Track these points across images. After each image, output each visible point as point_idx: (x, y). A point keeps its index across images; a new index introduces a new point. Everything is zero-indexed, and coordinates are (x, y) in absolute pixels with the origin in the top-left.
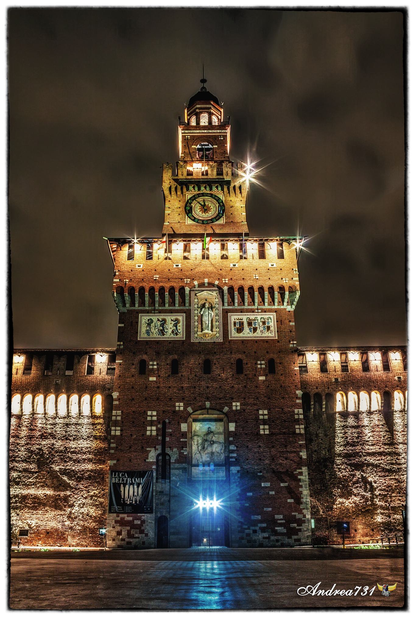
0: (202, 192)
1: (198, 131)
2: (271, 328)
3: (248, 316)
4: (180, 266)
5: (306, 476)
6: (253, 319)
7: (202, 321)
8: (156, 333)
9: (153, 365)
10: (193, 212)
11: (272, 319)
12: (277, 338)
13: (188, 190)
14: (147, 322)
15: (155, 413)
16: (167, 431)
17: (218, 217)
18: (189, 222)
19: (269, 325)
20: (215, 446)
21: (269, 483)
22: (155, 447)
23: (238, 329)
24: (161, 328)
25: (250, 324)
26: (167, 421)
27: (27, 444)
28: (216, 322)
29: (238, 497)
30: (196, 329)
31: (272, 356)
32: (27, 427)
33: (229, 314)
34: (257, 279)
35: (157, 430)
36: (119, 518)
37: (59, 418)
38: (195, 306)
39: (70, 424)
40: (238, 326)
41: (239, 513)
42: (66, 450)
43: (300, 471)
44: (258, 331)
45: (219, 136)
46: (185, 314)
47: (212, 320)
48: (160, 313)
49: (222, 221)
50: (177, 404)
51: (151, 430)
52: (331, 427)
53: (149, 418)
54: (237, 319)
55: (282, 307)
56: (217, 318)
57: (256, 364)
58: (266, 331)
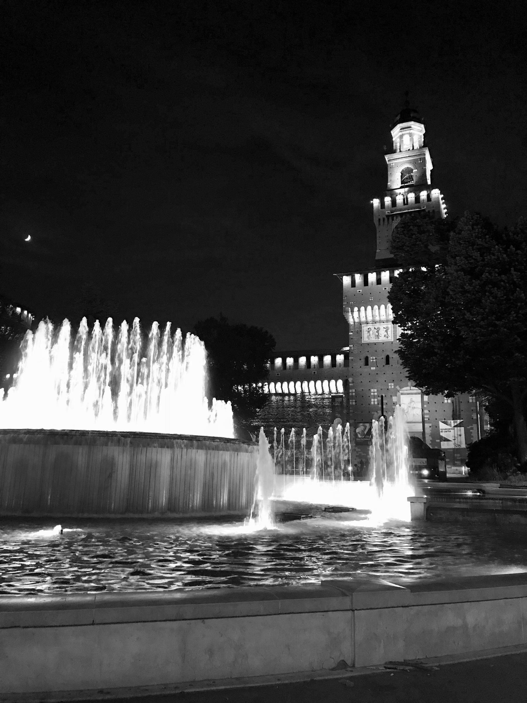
9: (373, 359)
14: (368, 330)
15: (376, 390)
20: (415, 410)
22: (377, 412)
24: (377, 334)
26: (384, 395)
27: (301, 411)
29: (431, 442)
32: (300, 401)
35: (378, 401)
37: (318, 395)
39: (325, 398)
42: (324, 414)
43: (472, 426)
45: (419, 160)
50: (390, 384)
51: (374, 401)
53: (372, 394)
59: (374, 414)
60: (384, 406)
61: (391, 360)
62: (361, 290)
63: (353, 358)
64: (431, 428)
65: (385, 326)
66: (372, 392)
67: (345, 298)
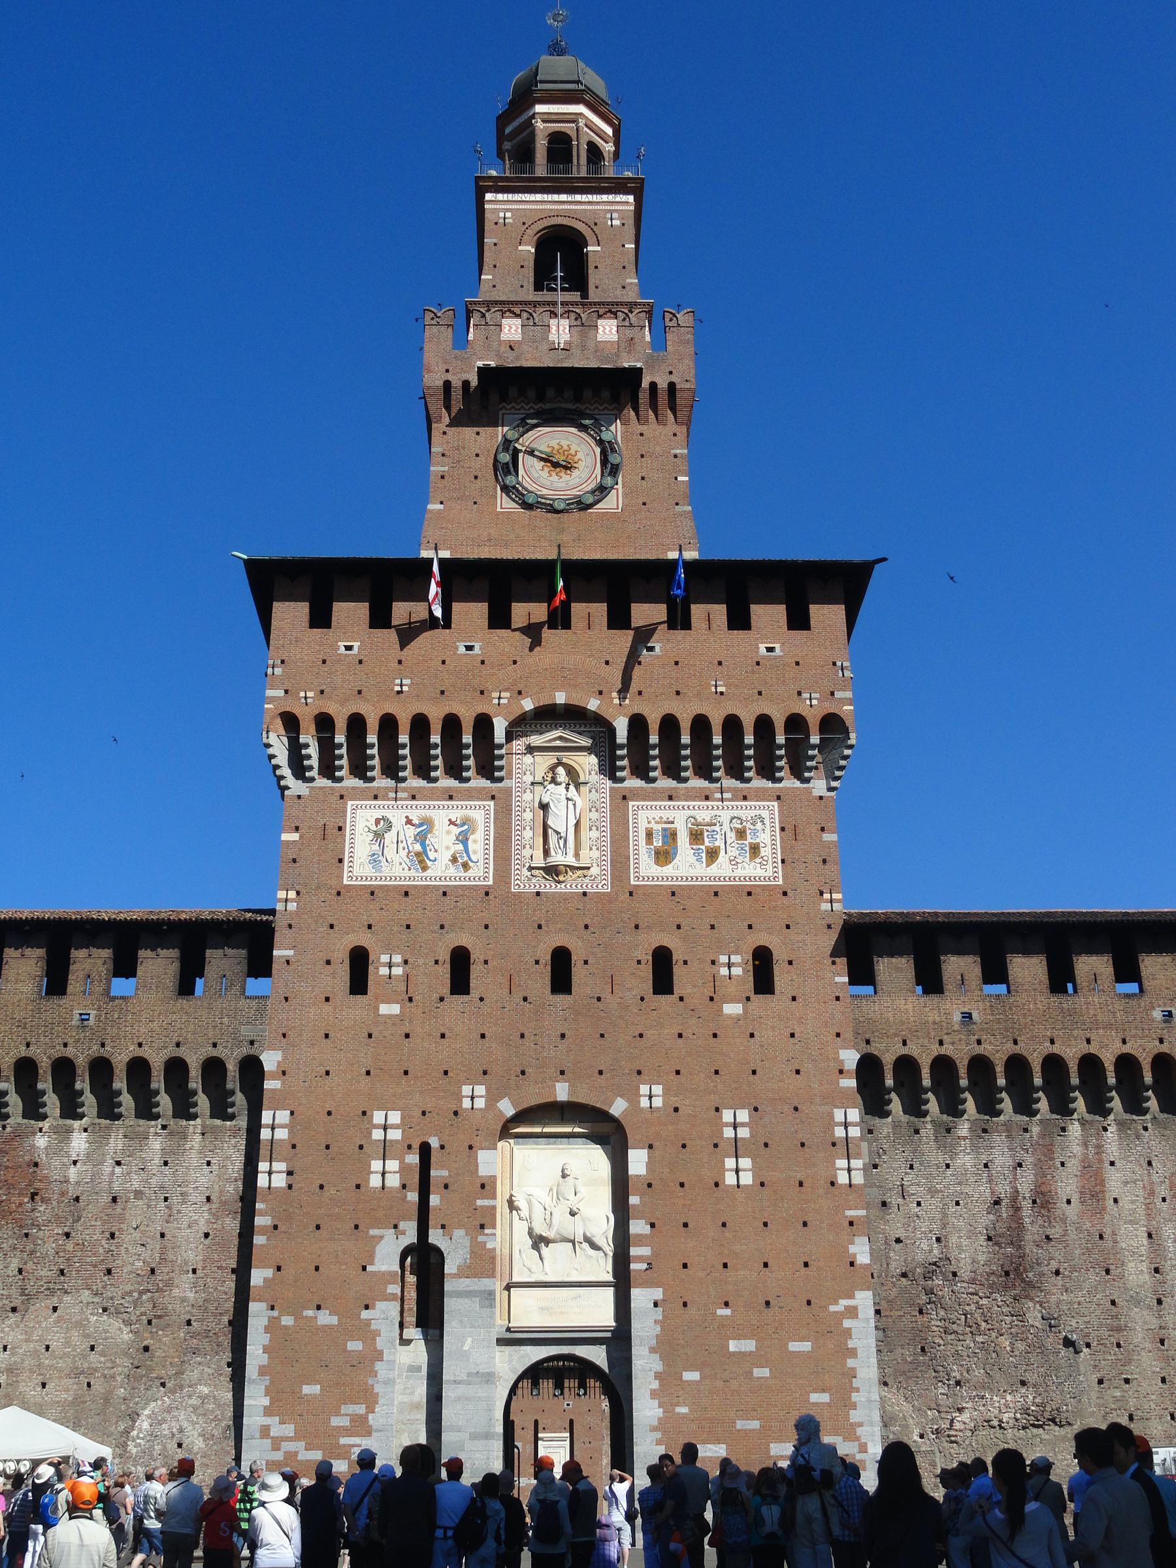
0: (548, 406)
1: (539, 197)
2: (762, 850)
3: (691, 813)
4: (477, 650)
5: (868, 1320)
6: (708, 820)
7: (545, 827)
8: (401, 864)
10: (521, 471)
11: (767, 821)
12: (781, 882)
13: (504, 398)
15: (395, 1117)
16: (433, 1173)
17: (602, 491)
18: (505, 504)
19: (758, 840)
21: (754, 1342)
22: (396, 1227)
24: (418, 847)
25: (696, 836)
26: (434, 1143)
28: (590, 829)
30: (527, 852)
31: (763, 939)
33: (631, 803)
34: (722, 693)
35: (404, 1169)
36: (283, 1450)
38: (525, 778)
40: (658, 842)
41: (658, 1435)
44: (722, 858)
45: (609, 216)
46: (492, 803)
47: (577, 825)
48: (414, 797)
49: (612, 503)
50: (466, 1090)
51: (383, 1174)
52: (948, 1166)
53: (377, 1134)
54: (657, 819)
55: (797, 784)
56: (594, 815)
57: (713, 962)
58: (747, 859)
59: (382, 1237)
60: (432, 1197)
61: (476, 972)
63: (291, 953)
64: (660, 1309)
65: (456, 815)
66: (377, 1127)
67: (278, 671)
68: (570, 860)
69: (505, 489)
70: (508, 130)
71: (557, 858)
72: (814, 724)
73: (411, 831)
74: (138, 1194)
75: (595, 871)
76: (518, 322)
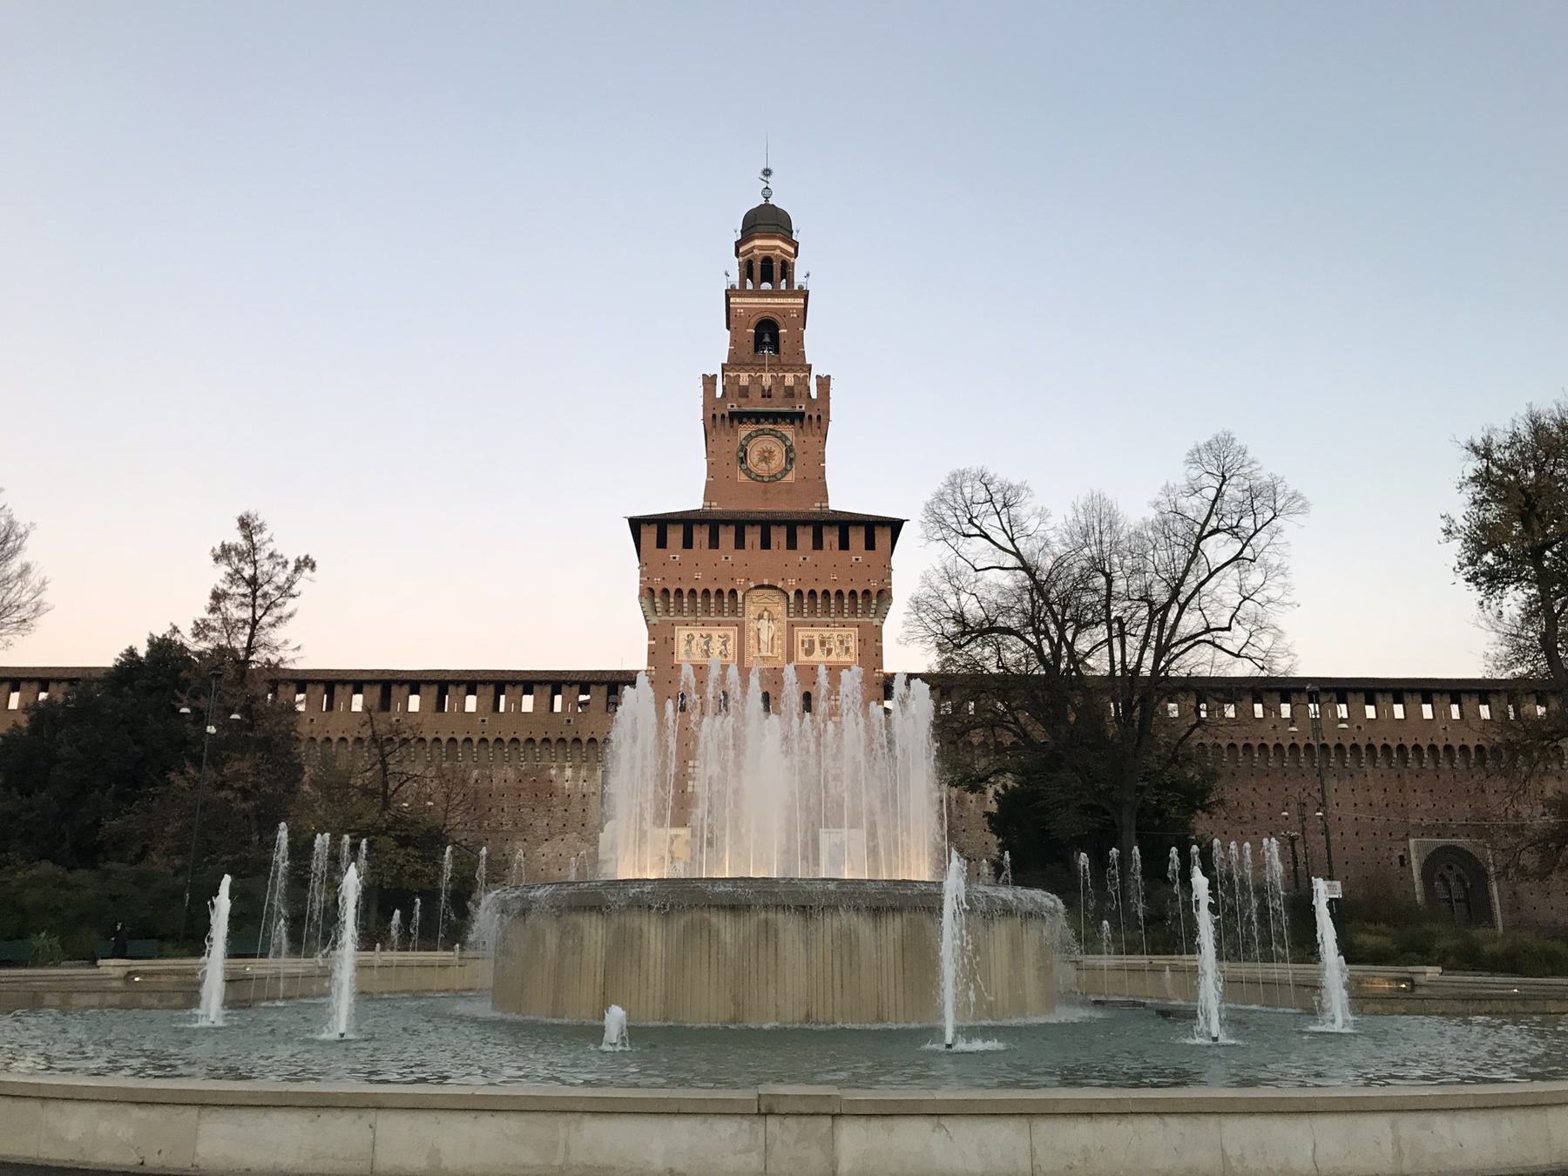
0: (761, 427)
4: (730, 559)
13: (741, 422)
17: (785, 471)
18: (742, 477)
23: (806, 650)
25: (823, 643)
40: (806, 646)
49: (790, 478)
55: (868, 620)
56: (780, 633)
62: (678, 556)
65: (721, 633)
68: (770, 654)
69: (744, 471)
70: (741, 250)
71: (764, 653)
72: (874, 593)
73: (703, 640)
74: (594, 794)
75: (780, 658)
76: (747, 374)
